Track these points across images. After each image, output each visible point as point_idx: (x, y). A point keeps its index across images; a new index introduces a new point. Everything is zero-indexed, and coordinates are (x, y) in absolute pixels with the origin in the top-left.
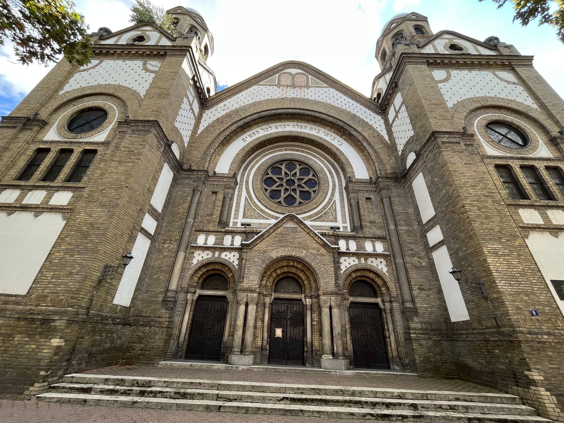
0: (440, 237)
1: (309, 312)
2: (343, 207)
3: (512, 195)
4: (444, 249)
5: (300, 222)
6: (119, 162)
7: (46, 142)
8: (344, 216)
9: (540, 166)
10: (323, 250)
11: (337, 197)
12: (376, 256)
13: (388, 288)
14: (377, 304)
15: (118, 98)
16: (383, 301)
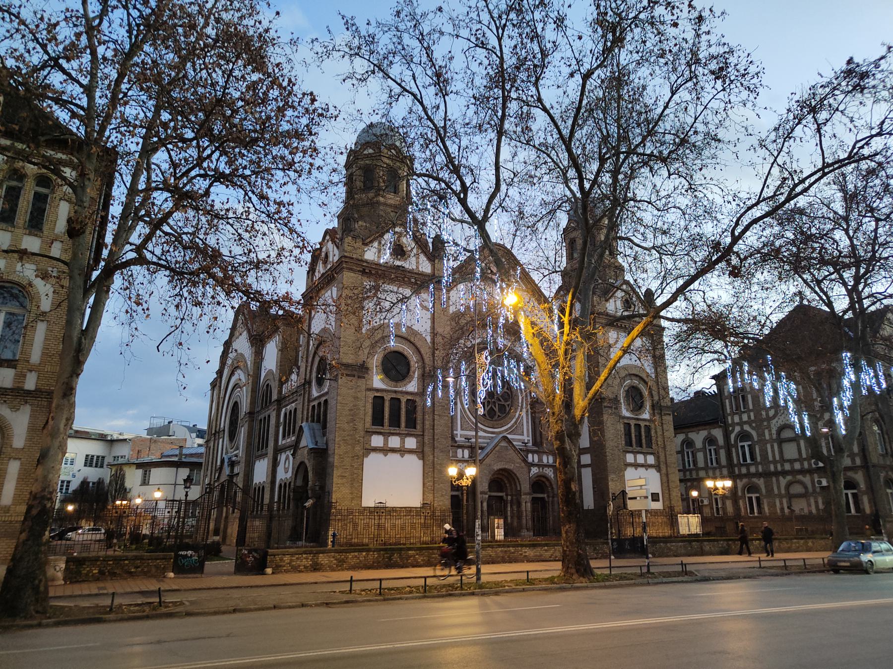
0: (589, 462)
1: (509, 505)
2: (528, 422)
3: (626, 445)
4: (589, 469)
5: (509, 441)
6: (439, 415)
7: (377, 390)
8: (528, 430)
9: (642, 424)
10: (523, 464)
11: (524, 414)
12: (548, 466)
13: (552, 488)
14: (543, 498)
15: (414, 344)
16: (548, 497)
